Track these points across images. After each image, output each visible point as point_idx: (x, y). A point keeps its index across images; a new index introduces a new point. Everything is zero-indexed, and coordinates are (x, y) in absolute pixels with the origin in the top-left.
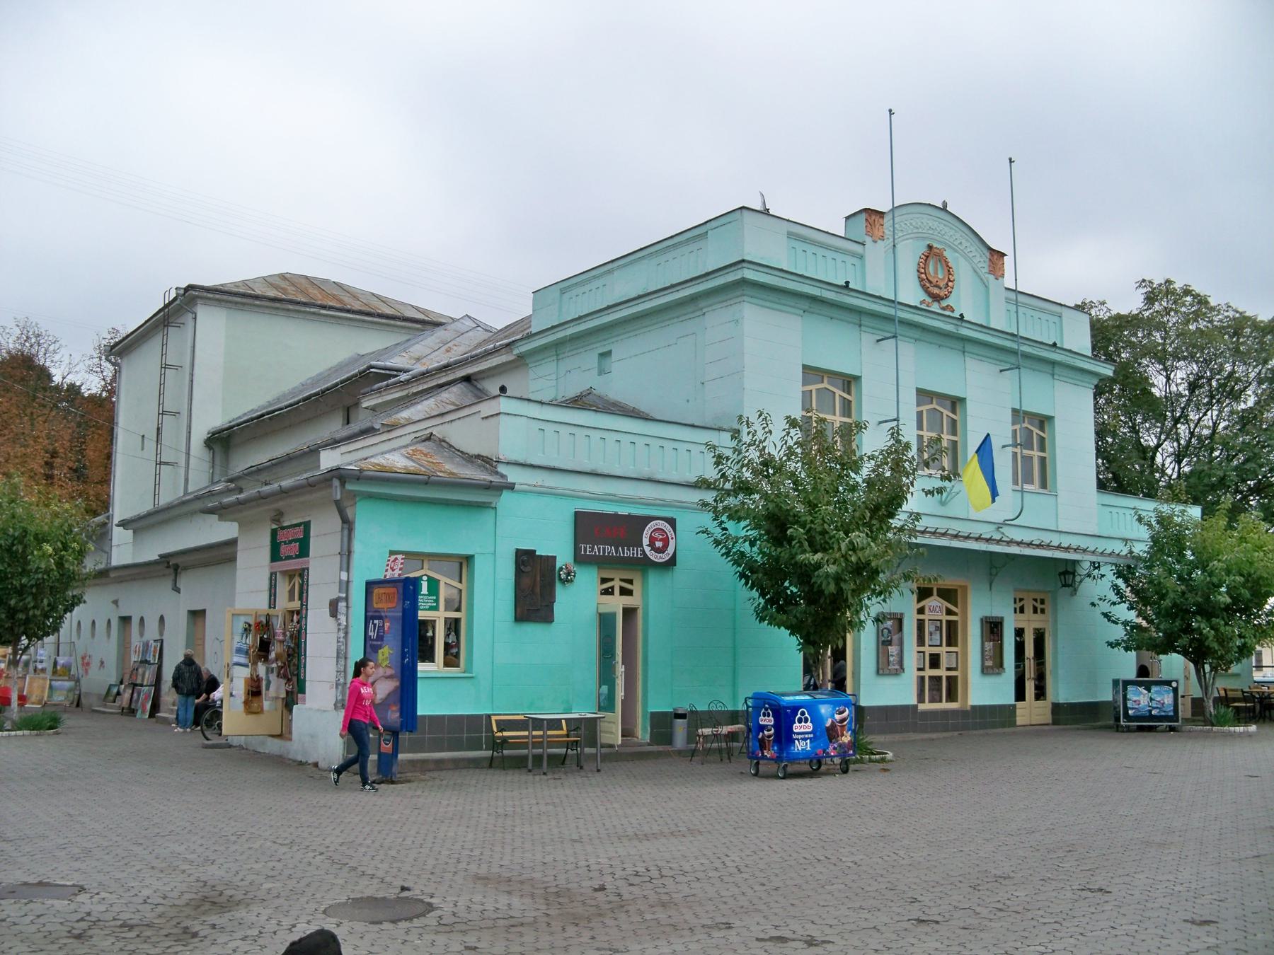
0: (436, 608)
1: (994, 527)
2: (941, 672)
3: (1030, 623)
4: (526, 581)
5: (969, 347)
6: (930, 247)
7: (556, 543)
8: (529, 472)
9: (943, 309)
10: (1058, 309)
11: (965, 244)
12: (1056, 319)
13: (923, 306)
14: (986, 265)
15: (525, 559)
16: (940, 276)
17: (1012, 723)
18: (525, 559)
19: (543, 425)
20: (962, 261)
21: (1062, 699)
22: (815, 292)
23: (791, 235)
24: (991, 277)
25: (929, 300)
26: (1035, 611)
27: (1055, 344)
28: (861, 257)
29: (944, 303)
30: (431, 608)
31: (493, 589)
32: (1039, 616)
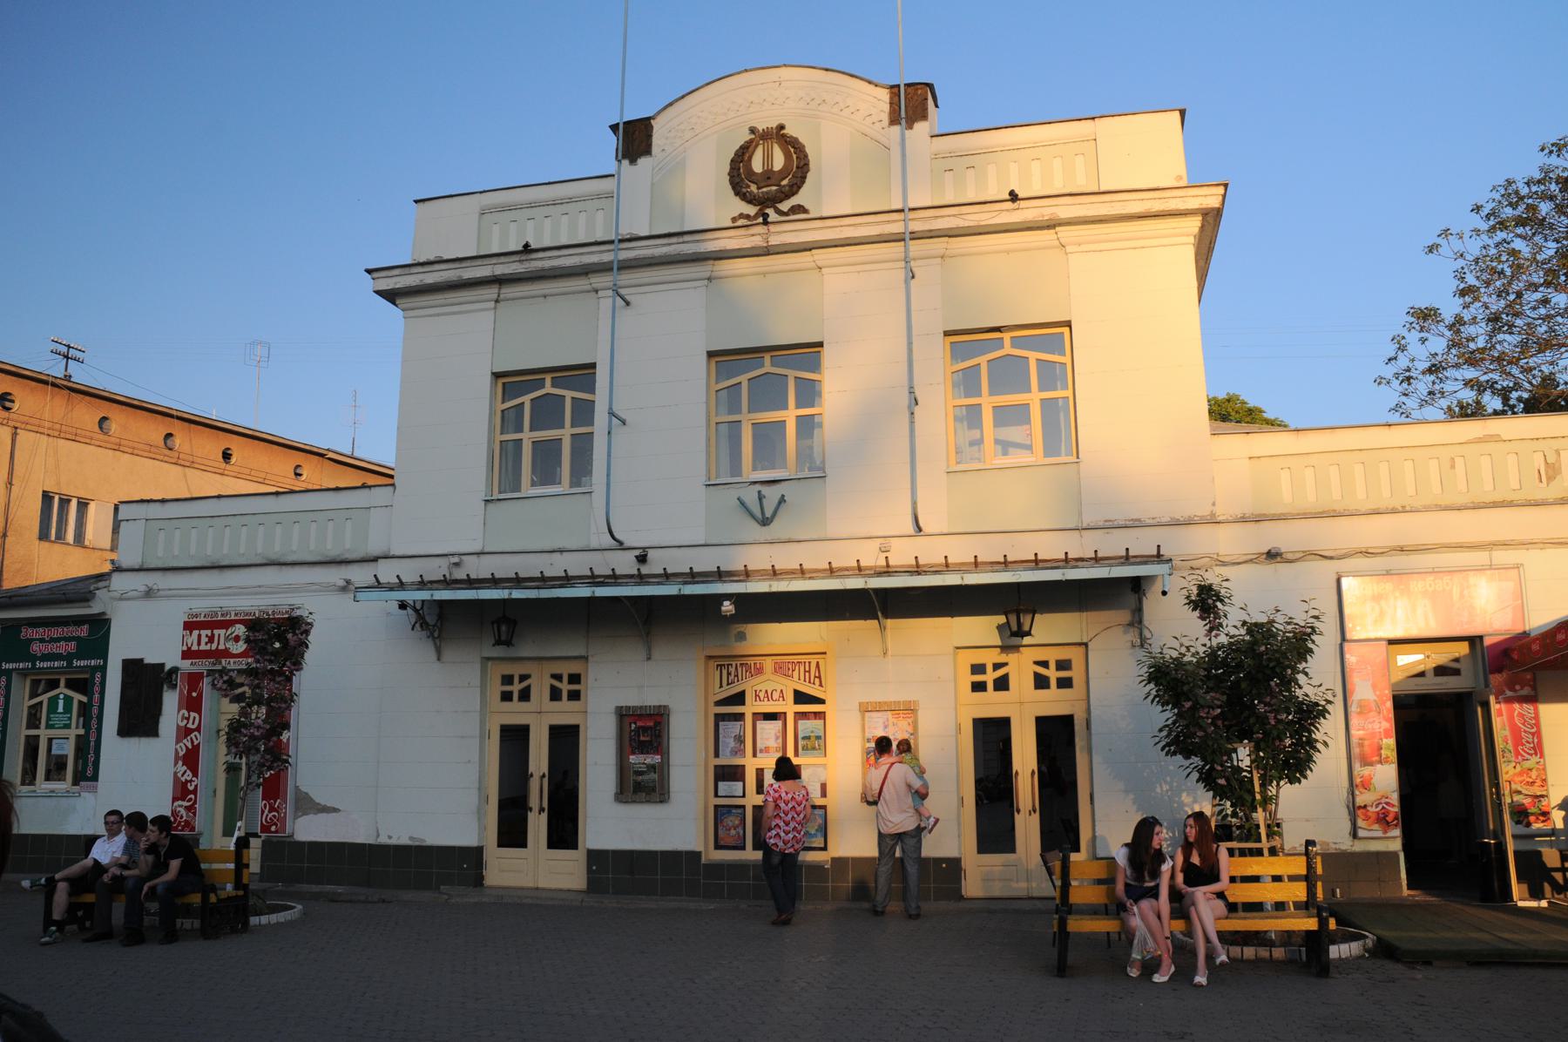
0: (67, 726)
6: (753, 130)
7: (165, 649)
9: (786, 214)
13: (741, 222)
18: (133, 668)
25: (751, 210)
27: (1014, 197)
29: (785, 206)
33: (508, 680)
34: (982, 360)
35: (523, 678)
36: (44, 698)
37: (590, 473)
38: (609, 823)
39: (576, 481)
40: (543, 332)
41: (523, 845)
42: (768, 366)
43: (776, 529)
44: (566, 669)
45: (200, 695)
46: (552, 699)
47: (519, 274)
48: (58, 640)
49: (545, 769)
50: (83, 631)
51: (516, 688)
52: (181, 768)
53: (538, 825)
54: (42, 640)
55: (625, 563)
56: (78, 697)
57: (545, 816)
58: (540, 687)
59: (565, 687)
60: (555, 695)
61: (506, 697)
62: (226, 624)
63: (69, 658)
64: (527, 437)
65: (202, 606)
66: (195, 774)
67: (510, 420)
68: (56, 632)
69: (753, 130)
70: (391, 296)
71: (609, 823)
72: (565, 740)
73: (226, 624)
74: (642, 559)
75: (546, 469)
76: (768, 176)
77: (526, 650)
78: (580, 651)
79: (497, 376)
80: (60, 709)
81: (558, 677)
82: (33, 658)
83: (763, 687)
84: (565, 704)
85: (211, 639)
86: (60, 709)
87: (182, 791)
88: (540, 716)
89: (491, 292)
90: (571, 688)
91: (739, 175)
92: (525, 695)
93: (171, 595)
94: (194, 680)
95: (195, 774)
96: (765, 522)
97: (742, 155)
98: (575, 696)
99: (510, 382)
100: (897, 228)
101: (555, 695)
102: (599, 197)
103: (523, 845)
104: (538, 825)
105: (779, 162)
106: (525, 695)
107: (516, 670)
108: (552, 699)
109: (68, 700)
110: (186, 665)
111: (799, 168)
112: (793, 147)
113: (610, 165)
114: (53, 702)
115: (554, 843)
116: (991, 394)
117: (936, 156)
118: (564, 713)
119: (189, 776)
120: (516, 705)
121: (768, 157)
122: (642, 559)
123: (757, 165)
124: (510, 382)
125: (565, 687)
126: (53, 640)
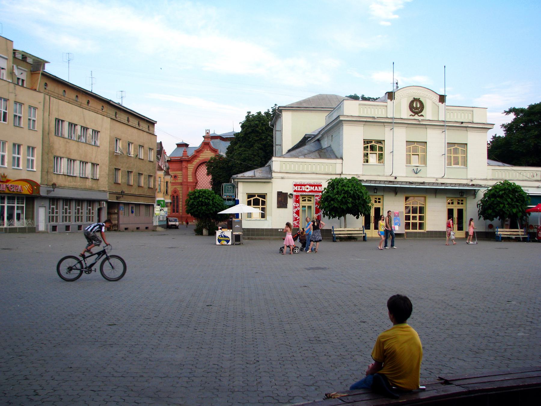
3: (455, 207)
4: (280, 199)
5: (427, 127)
7: (288, 189)
10: (472, 109)
11: (429, 95)
15: (280, 194)
16: (418, 106)
18: (280, 194)
22: (365, 120)
24: (440, 103)
25: (413, 114)
26: (458, 203)
28: (386, 106)
29: (420, 114)
31: (272, 201)
32: (460, 205)
34: (452, 148)
40: (374, 134)
41: (369, 229)
42: (415, 145)
43: (418, 175)
44: (378, 197)
45: (299, 200)
52: (295, 214)
53: (372, 225)
55: (392, 179)
59: (378, 200)
62: (305, 185)
65: (298, 182)
66: (299, 216)
73: (305, 185)
74: (396, 178)
76: (417, 108)
77: (378, 194)
85: (301, 188)
87: (296, 219)
89: (364, 123)
91: (411, 107)
93: (288, 178)
94: (297, 196)
95: (299, 216)
96: (416, 173)
97: (412, 102)
98: (379, 202)
101: (376, 202)
102: (383, 106)
103: (369, 229)
104: (372, 225)
105: (418, 106)
110: (295, 193)
112: (421, 103)
115: (375, 229)
119: (297, 216)
121: (416, 105)
123: (415, 106)
125: (378, 200)
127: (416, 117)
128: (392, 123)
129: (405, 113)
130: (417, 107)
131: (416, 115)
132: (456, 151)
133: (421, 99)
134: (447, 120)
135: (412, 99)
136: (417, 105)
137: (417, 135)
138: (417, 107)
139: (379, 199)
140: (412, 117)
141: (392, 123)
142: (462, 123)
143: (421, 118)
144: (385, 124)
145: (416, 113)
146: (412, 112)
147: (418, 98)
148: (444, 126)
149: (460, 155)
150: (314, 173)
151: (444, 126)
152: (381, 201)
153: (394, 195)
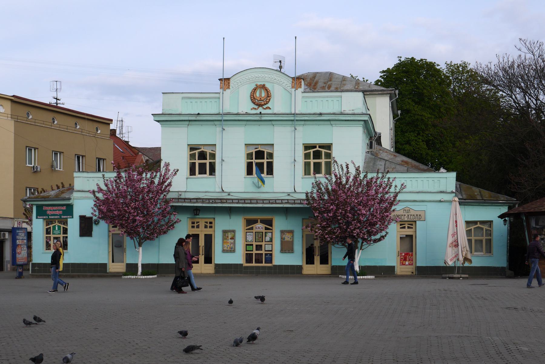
1: (286, 194)
2: (263, 252)
5: (274, 123)
8: (83, 193)
9: (265, 109)
12: (339, 99)
14: (290, 85)
17: (301, 273)
18: (83, 218)
19: (88, 179)
20: (276, 86)
21: (333, 264)
22: (186, 118)
23: (183, 98)
25: (256, 107)
29: (265, 107)
30: (59, 234)
33: (193, 223)
35: (197, 222)
36: (51, 226)
37: (214, 172)
38: (220, 258)
39: (211, 174)
40: (202, 136)
44: (209, 221)
46: (205, 227)
47: (196, 120)
48: (56, 210)
49: (203, 244)
50: (64, 208)
51: (195, 225)
54: (50, 210)
55: (224, 196)
56: (62, 226)
57: (203, 256)
58: (202, 224)
59: (208, 225)
60: (206, 227)
61: (193, 227)
63: (60, 215)
64: (197, 162)
67: (192, 156)
68: (55, 208)
69: (256, 85)
70: (158, 121)
71: (220, 258)
72: (209, 239)
75: (202, 171)
78: (213, 217)
79: (188, 145)
80: (57, 229)
81: (207, 222)
82: (48, 215)
83: (258, 226)
84: (208, 229)
86: (57, 229)
88: (202, 232)
89: (187, 123)
90: (211, 225)
92: (198, 227)
98: (211, 227)
99: (192, 148)
100: (292, 118)
101: (206, 227)
102: (215, 98)
106: (198, 227)
107: (196, 221)
108: (205, 227)
109: (59, 227)
111: (269, 95)
113: (218, 90)
114: (54, 227)
116: (314, 159)
117: (303, 97)
118: (209, 231)
120: (195, 229)
122: (229, 195)
123: (258, 94)
124: (192, 148)
125: (208, 225)
126: (54, 210)
127: (260, 110)
128: (223, 120)
129: (245, 106)
130: (261, 97)
131: (260, 108)
132: (317, 155)
133: (268, 86)
134: (297, 112)
135: (254, 86)
136: (260, 94)
137: (260, 135)
138: (261, 97)
139: (211, 223)
140: (254, 112)
141: (223, 120)
142: (321, 114)
143: (268, 111)
144: (332, 122)
145: (260, 105)
146: (254, 103)
147: (262, 84)
148: (294, 120)
149: (323, 161)
150: (441, 192)
151: (294, 120)
152: (213, 225)
153: (229, 217)
